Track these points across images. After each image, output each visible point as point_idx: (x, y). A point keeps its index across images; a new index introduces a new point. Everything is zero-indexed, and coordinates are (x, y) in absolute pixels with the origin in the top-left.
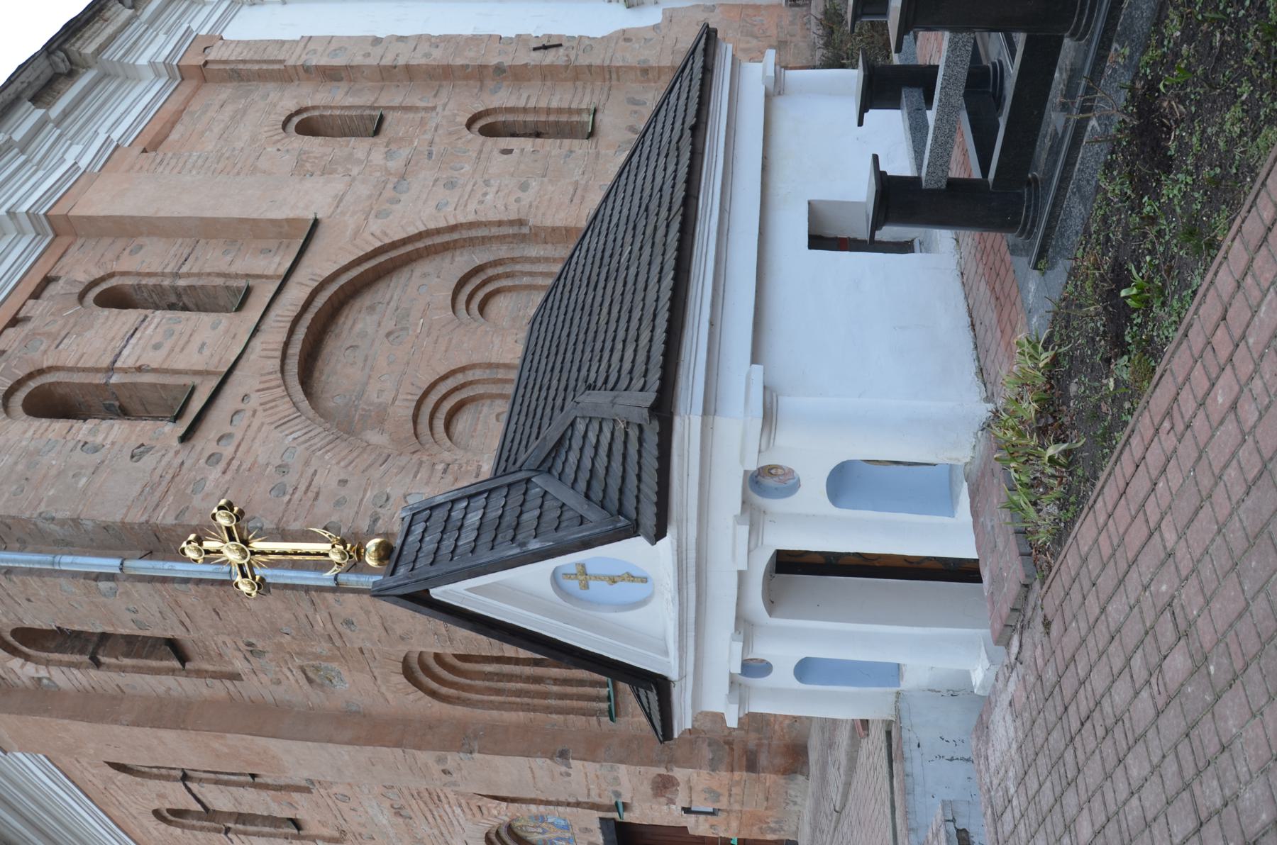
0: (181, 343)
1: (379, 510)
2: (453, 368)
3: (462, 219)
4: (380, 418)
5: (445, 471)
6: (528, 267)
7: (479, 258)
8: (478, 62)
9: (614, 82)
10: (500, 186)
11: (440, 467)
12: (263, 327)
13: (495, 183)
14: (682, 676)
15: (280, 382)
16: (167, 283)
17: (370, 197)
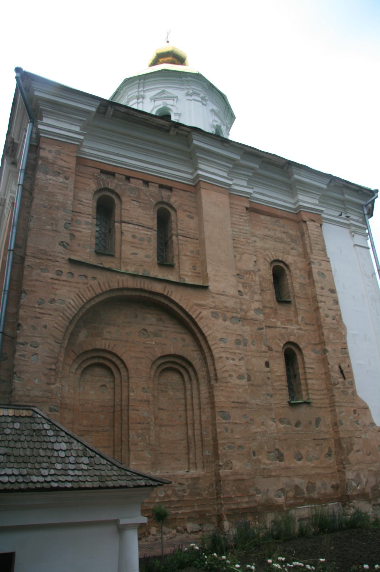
0: (137, 245)
1: (29, 344)
2: (125, 362)
3: (214, 352)
5: (50, 369)
6: (195, 386)
7: (197, 363)
10: (240, 366)
11: (53, 367)
13: (242, 363)
15: (104, 290)
17: (226, 307)
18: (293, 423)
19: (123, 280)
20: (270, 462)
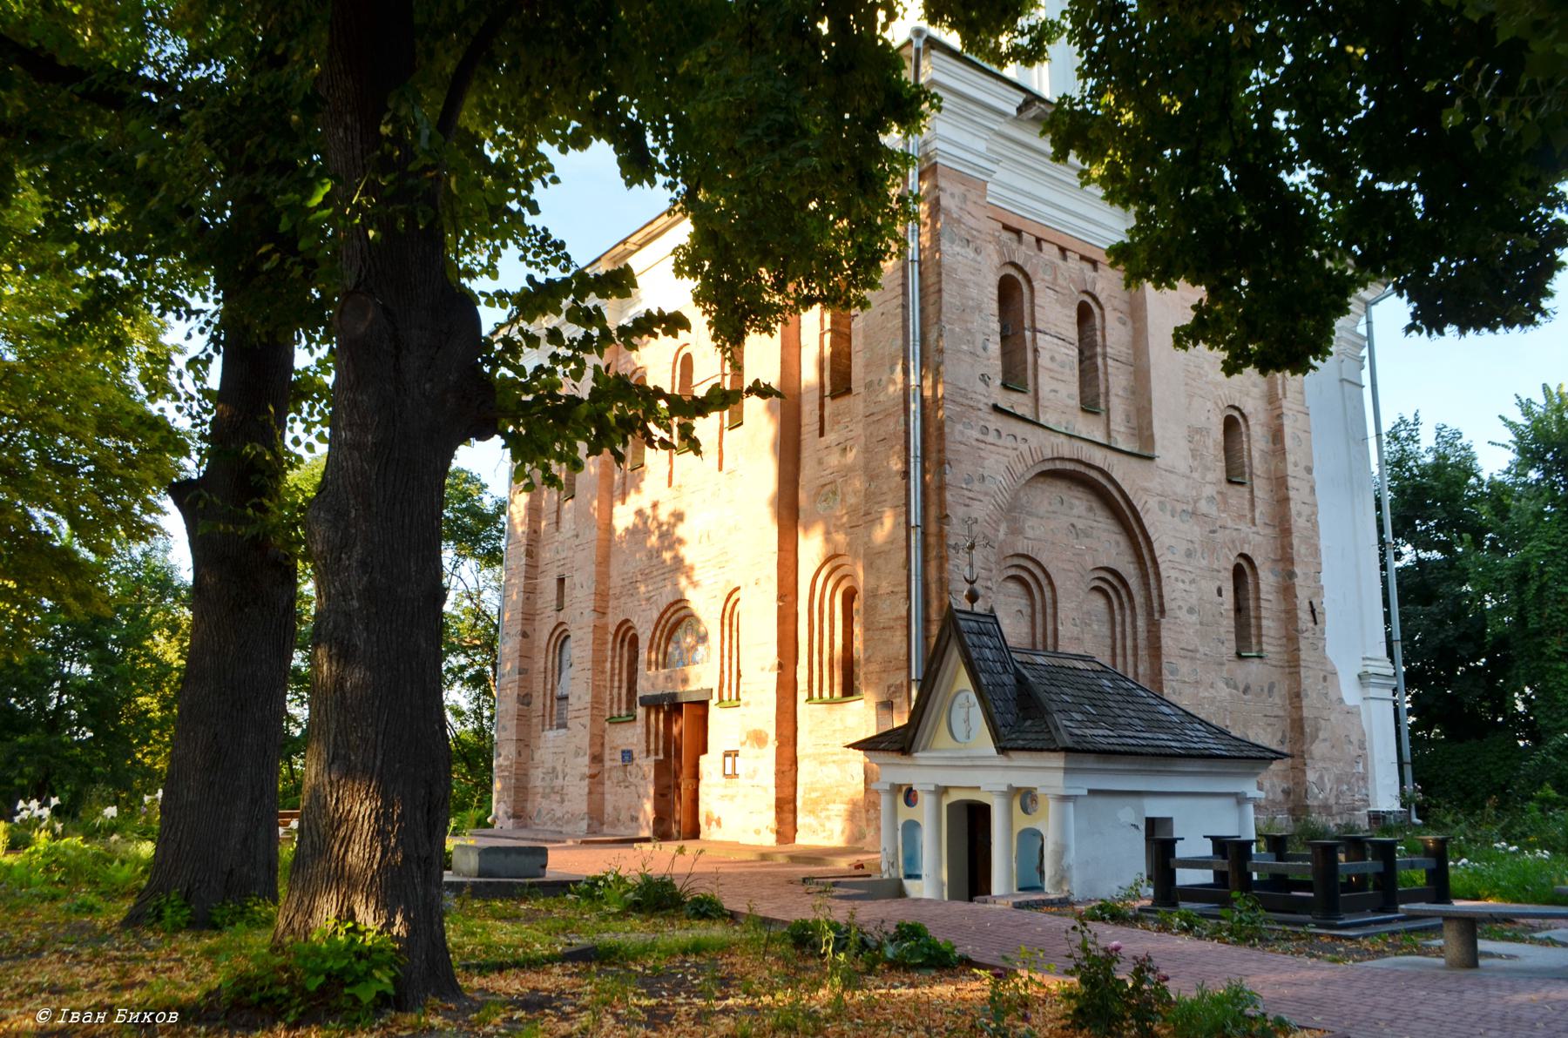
0: (1056, 376)
3: (1162, 567)
4: (1015, 531)
6: (1128, 620)
7: (1134, 583)
8: (1295, 557)
9: (1287, 670)
11: (989, 584)
12: (1073, 440)
13: (1193, 588)
16: (1099, 350)
17: (1175, 494)
18: (1241, 687)
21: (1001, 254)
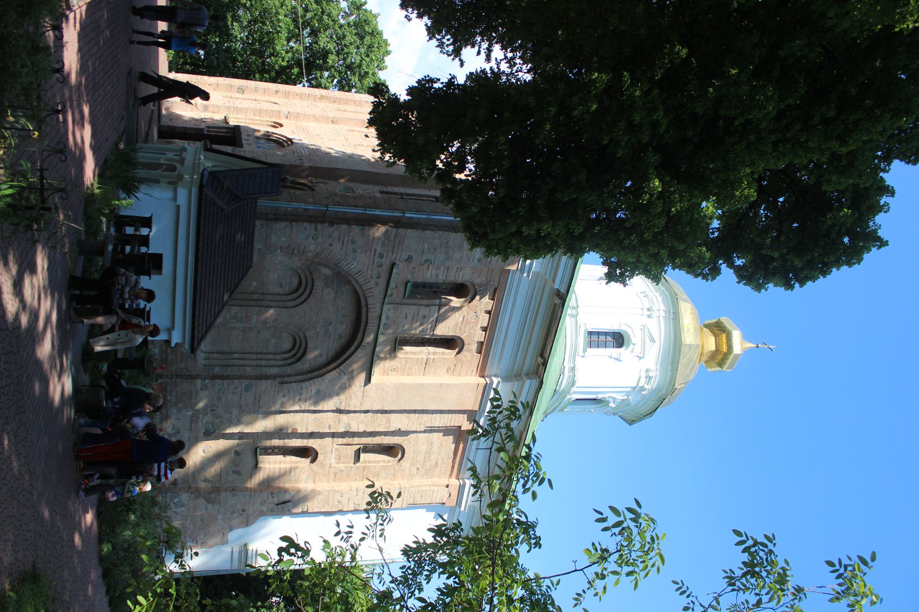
2: (302, 306)
5: (294, 250)
6: (277, 363)
7: (299, 366)
11: (296, 251)
12: (378, 320)
14: (200, 152)
15: (366, 292)
19: (375, 308)
20: (204, 423)
21: (481, 286)
